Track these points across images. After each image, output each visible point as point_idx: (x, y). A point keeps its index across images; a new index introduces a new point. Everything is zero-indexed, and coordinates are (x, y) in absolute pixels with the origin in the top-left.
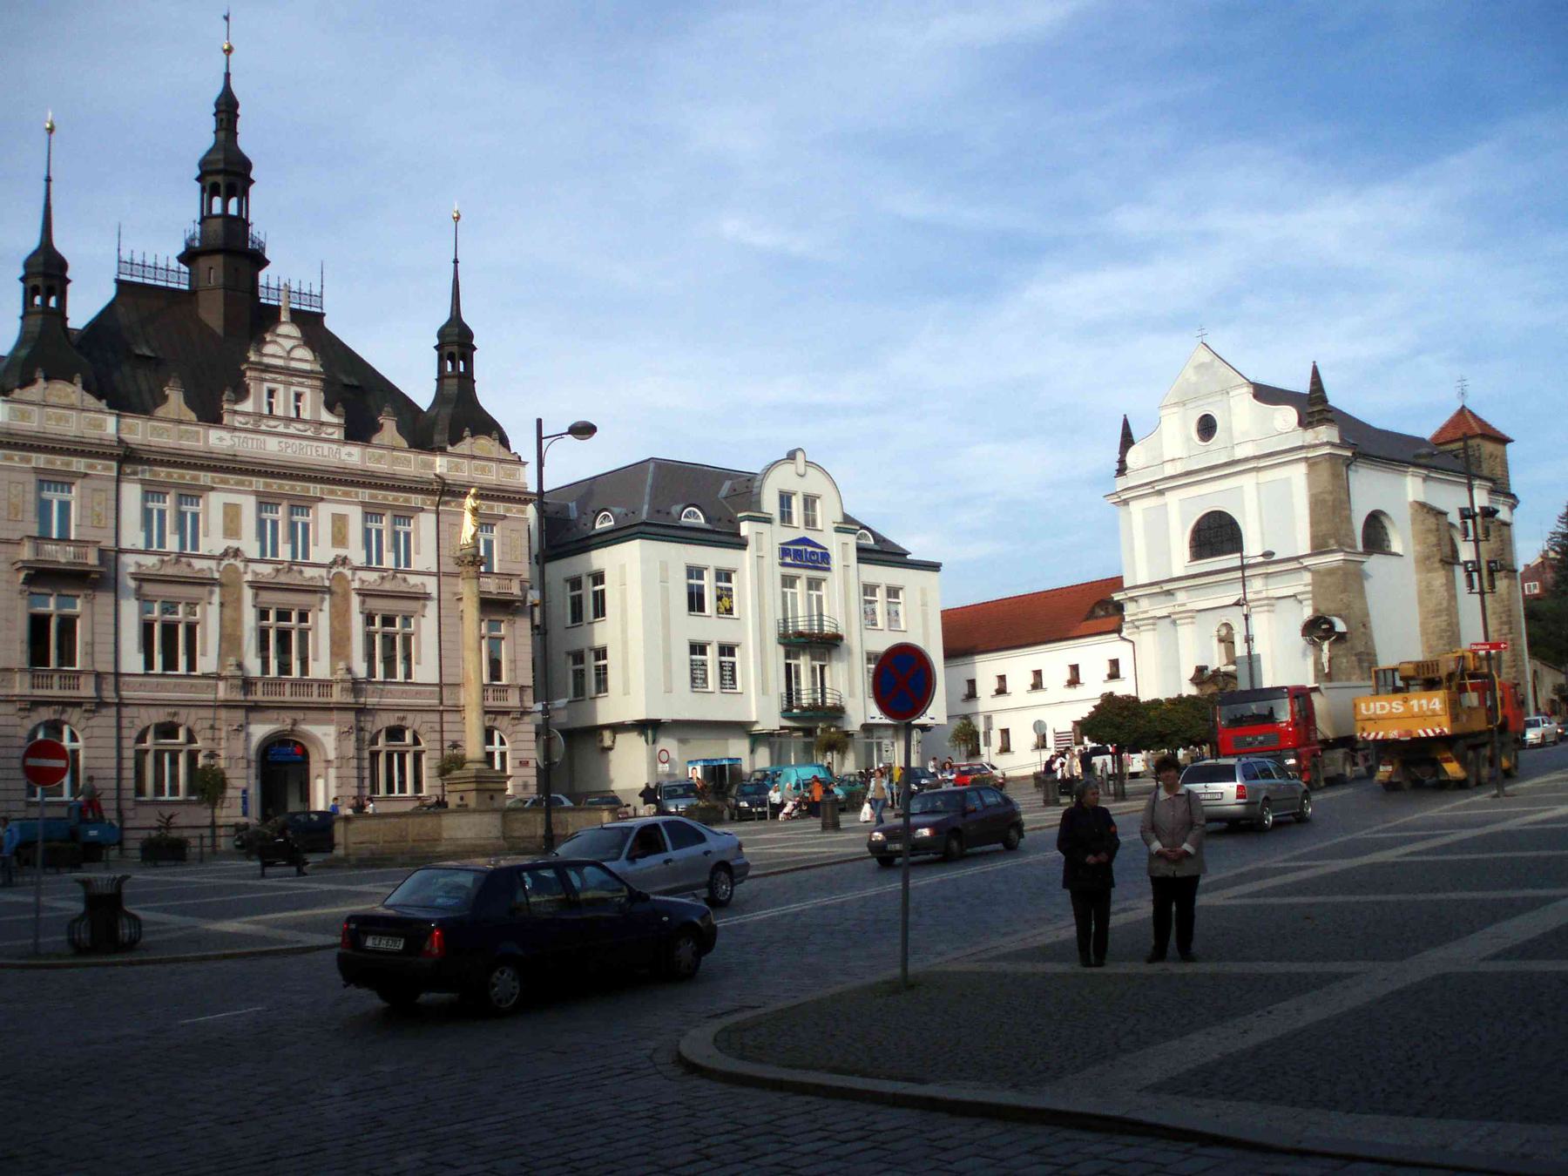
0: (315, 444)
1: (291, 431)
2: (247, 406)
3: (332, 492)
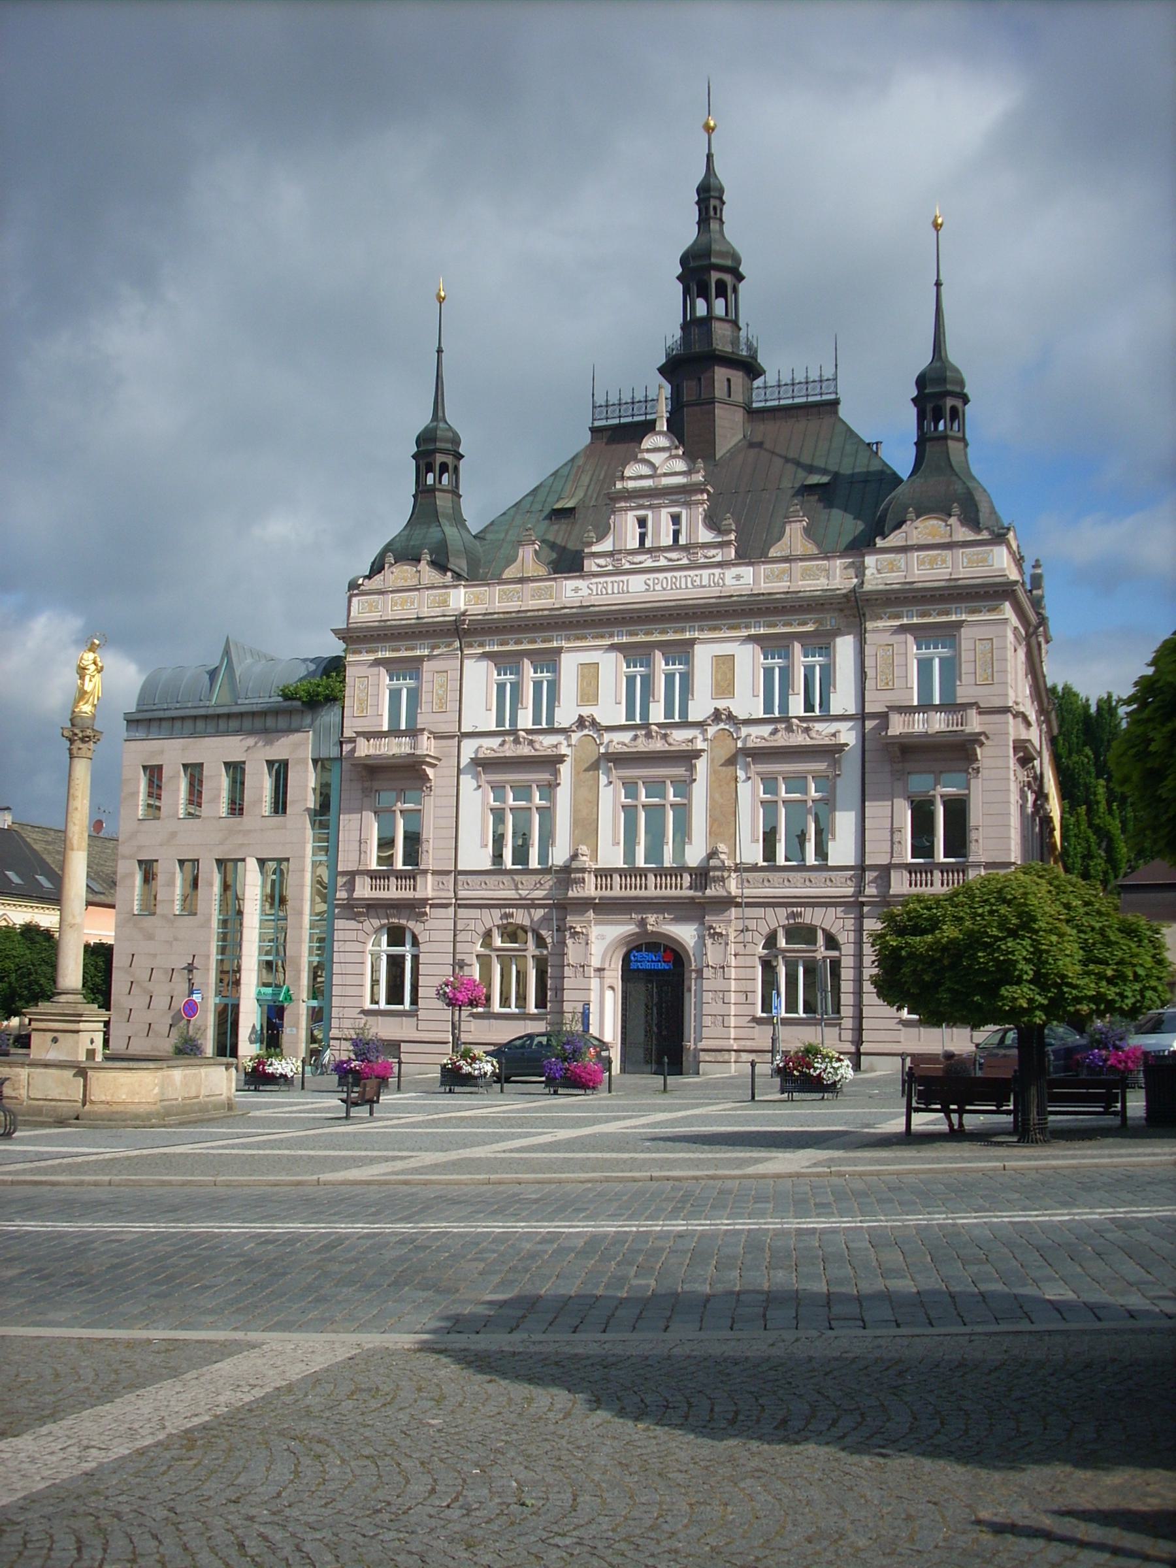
0: (692, 573)
1: (663, 562)
2: (606, 545)
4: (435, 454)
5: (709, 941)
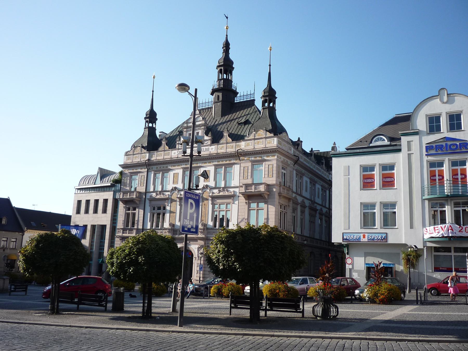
4: (152, 117)
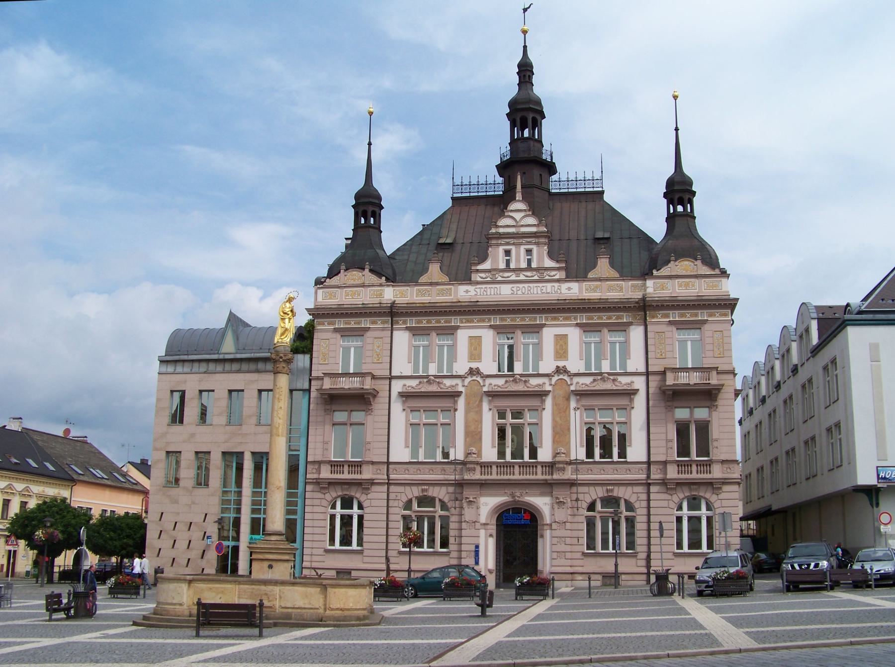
0: (541, 285)
1: (522, 277)
3: (555, 319)
4: (368, 205)
5: (556, 506)
